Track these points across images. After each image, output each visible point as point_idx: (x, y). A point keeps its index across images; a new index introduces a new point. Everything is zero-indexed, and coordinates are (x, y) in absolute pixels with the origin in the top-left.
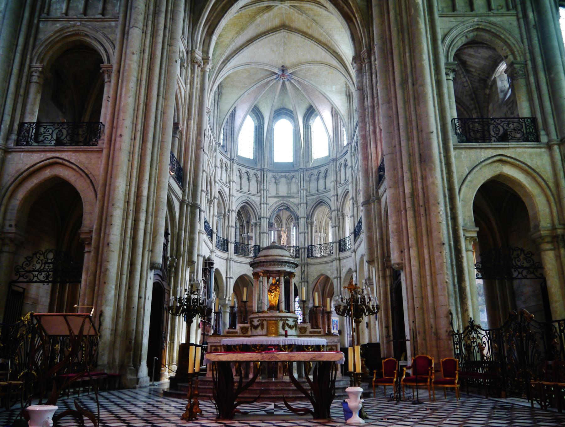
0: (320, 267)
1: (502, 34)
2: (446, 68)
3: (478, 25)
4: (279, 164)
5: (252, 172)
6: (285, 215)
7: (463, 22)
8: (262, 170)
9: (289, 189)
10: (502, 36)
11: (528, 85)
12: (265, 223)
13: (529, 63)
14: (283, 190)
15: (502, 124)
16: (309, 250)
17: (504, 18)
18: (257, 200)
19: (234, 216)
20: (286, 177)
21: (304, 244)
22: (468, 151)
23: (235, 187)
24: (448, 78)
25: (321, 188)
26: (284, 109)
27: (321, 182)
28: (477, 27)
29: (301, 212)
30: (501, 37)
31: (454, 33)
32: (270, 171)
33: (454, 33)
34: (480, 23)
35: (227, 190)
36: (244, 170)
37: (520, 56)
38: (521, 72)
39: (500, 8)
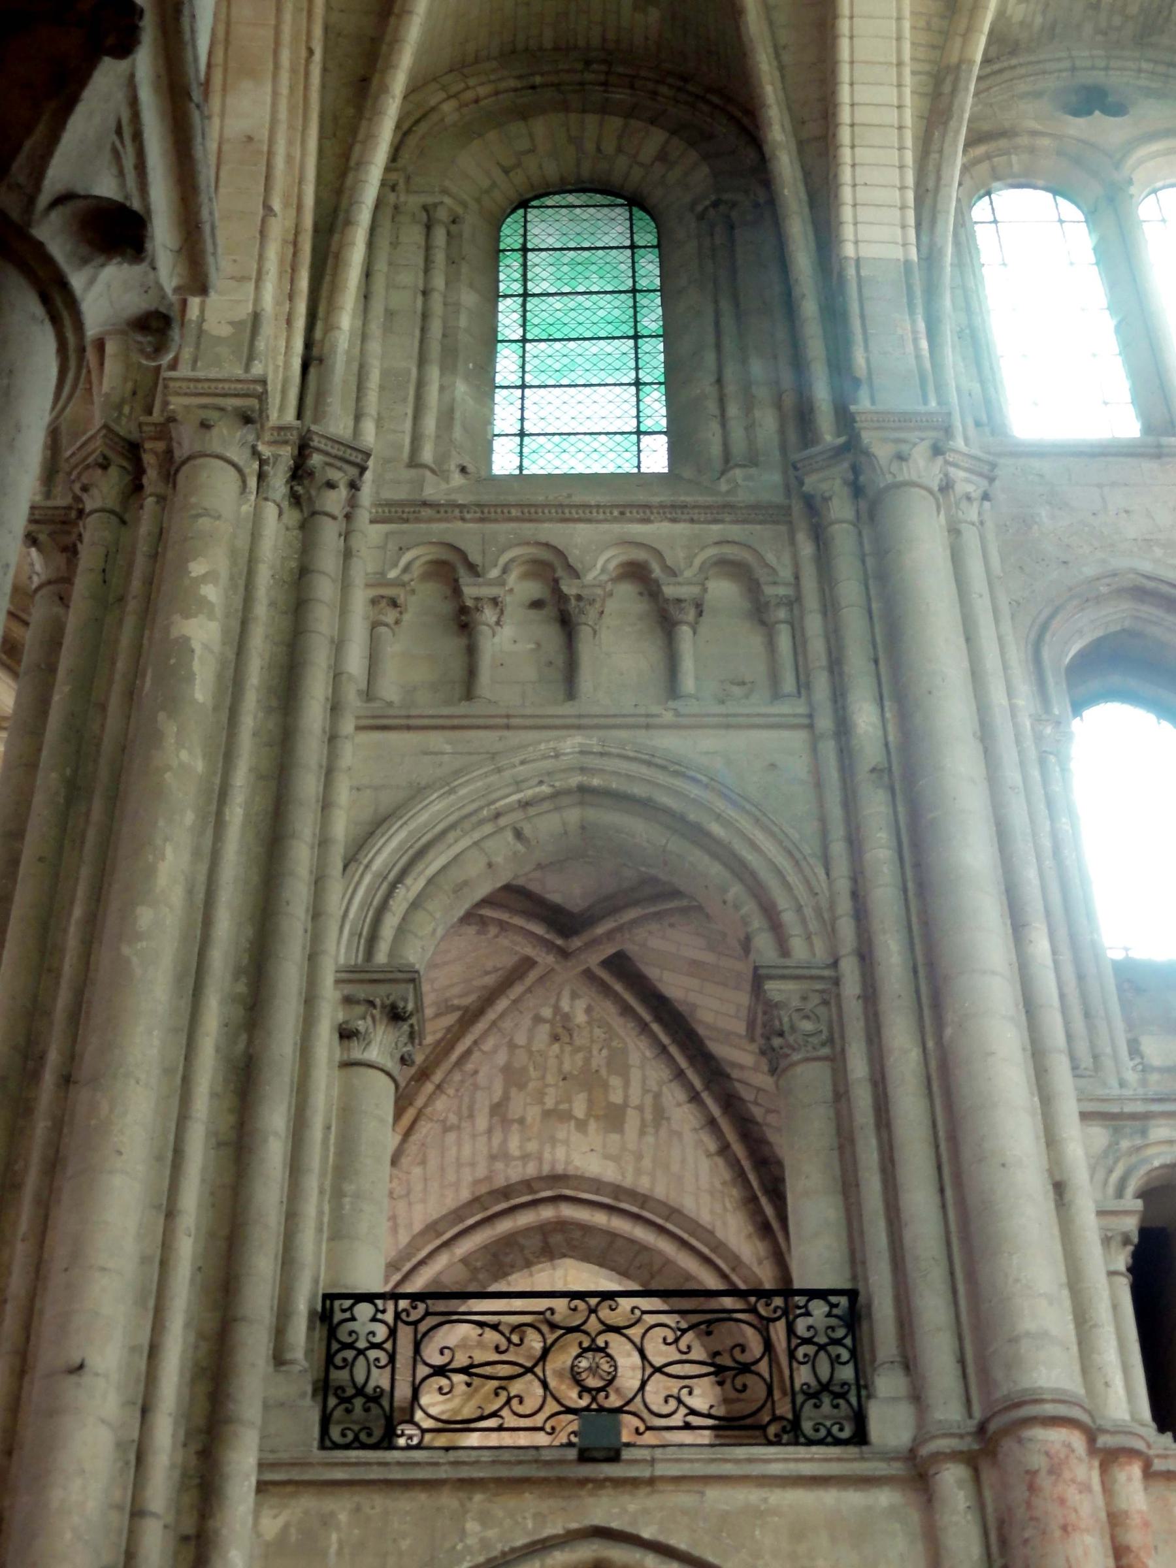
1: (718, 817)
2: (348, 1000)
3: (583, 770)
7: (493, 756)
10: (716, 829)
11: (841, 1095)
13: (849, 968)
15: (635, 1332)
17: (739, 741)
22: (376, 1503)
24: (357, 1054)
28: (575, 780)
30: (708, 835)
31: (433, 811)
33: (433, 811)
34: (597, 762)
37: (809, 938)
38: (807, 1026)
39: (737, 691)
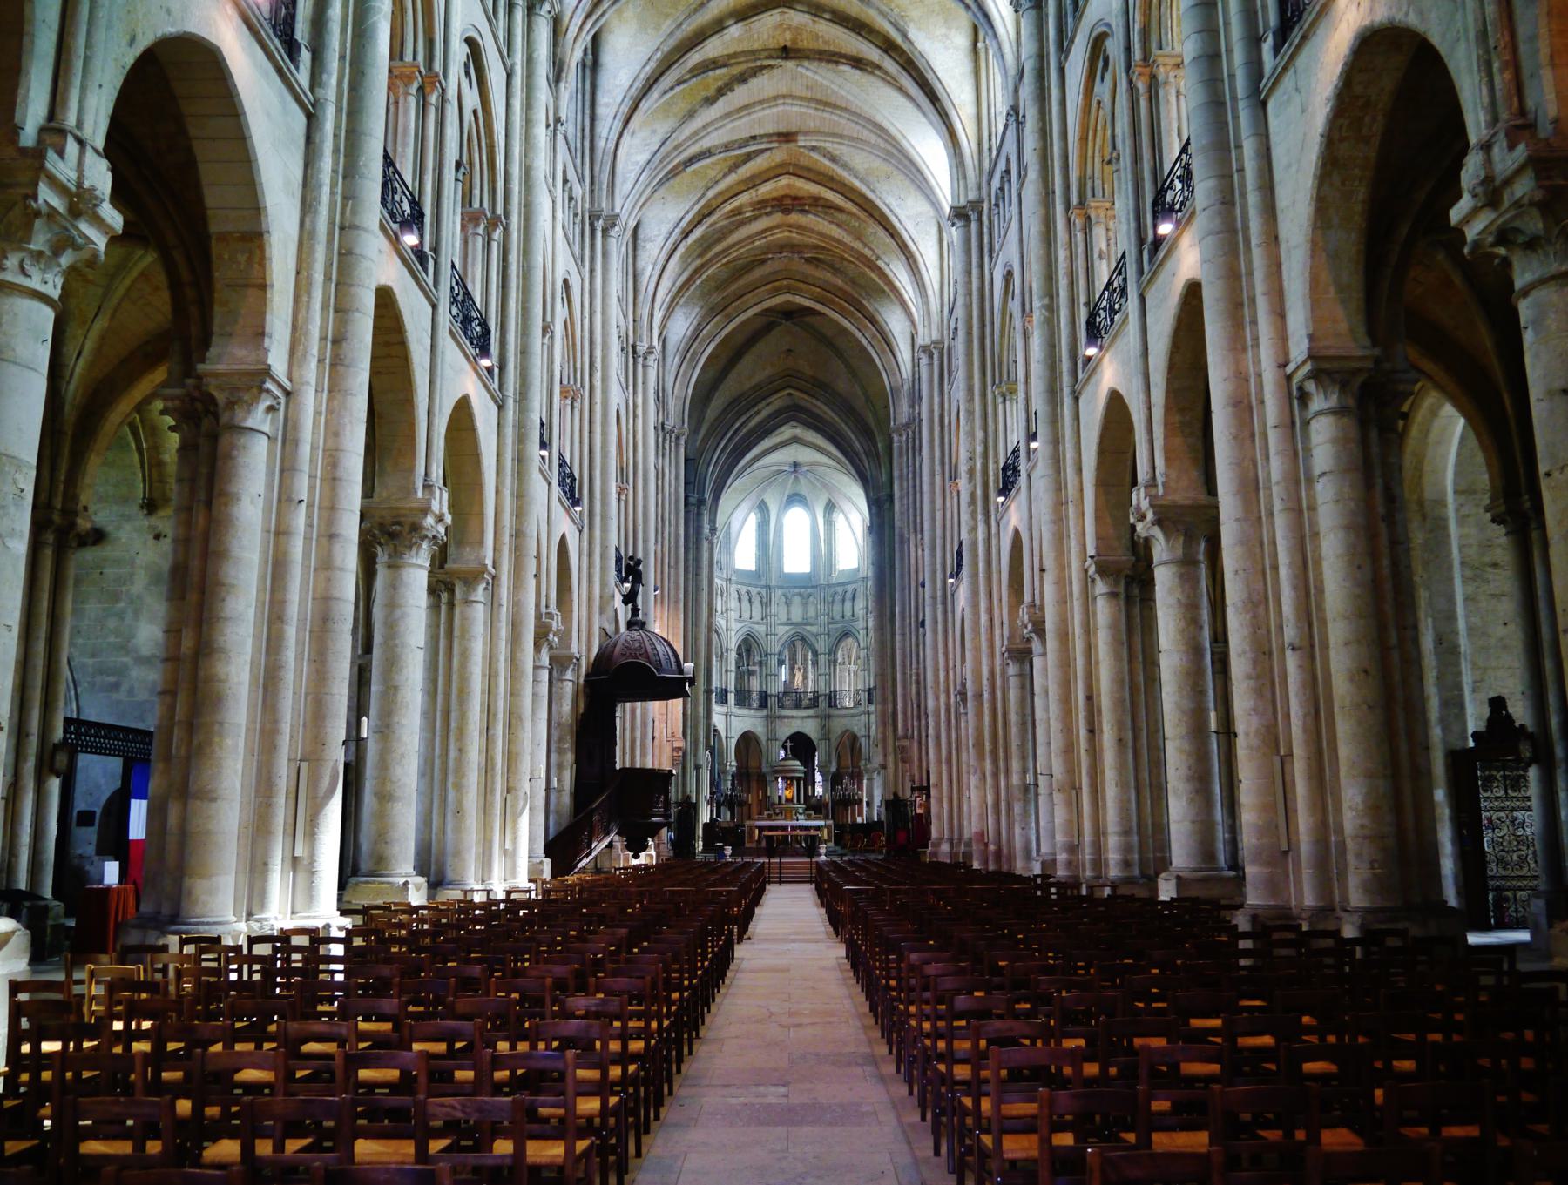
0: (845, 721)
4: (790, 575)
5: (754, 591)
6: (799, 644)
8: (768, 587)
9: (805, 612)
12: (774, 661)
14: (797, 615)
16: (832, 699)
18: (762, 629)
19: (733, 656)
20: (800, 595)
21: (825, 690)
23: (734, 615)
25: (848, 613)
26: (796, 494)
27: (848, 605)
29: (822, 645)
32: (781, 588)
35: (723, 622)
36: (744, 589)
